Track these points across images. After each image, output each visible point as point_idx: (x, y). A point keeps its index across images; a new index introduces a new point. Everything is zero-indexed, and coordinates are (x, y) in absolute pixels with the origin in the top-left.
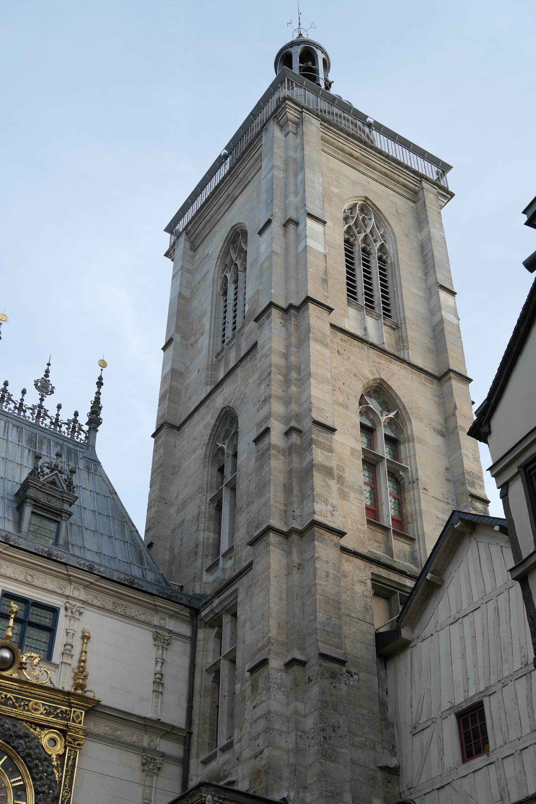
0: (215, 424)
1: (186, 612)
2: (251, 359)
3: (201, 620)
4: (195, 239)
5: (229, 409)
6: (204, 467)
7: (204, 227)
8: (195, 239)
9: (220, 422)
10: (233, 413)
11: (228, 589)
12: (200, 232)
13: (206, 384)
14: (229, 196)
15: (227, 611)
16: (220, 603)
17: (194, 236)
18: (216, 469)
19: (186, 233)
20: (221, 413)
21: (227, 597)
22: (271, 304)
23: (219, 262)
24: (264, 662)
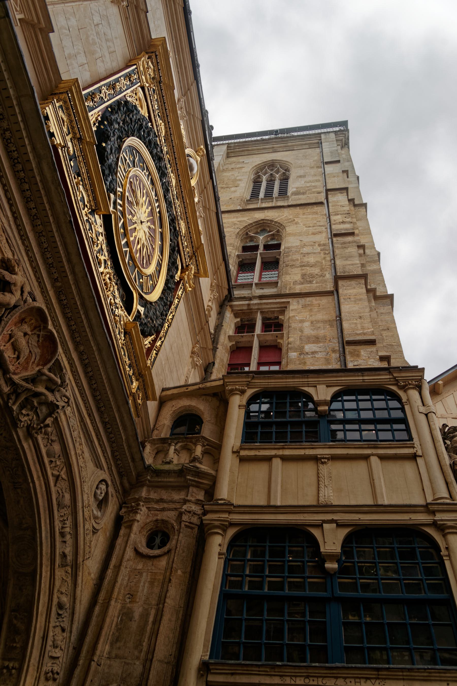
0: (251, 224)
1: (226, 292)
2: (300, 209)
3: (231, 306)
4: (231, 152)
5: (269, 222)
6: (236, 237)
7: (243, 151)
8: (231, 152)
9: (256, 225)
10: (269, 226)
11: (276, 299)
12: (237, 152)
13: (240, 205)
14: (273, 148)
15: (262, 313)
16: (258, 304)
17: (232, 150)
18: (242, 245)
19: (228, 147)
20: (260, 221)
21: (271, 303)
22: (346, 189)
23: (255, 168)
24: (372, 342)
